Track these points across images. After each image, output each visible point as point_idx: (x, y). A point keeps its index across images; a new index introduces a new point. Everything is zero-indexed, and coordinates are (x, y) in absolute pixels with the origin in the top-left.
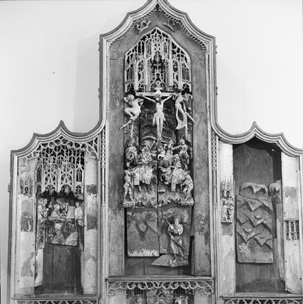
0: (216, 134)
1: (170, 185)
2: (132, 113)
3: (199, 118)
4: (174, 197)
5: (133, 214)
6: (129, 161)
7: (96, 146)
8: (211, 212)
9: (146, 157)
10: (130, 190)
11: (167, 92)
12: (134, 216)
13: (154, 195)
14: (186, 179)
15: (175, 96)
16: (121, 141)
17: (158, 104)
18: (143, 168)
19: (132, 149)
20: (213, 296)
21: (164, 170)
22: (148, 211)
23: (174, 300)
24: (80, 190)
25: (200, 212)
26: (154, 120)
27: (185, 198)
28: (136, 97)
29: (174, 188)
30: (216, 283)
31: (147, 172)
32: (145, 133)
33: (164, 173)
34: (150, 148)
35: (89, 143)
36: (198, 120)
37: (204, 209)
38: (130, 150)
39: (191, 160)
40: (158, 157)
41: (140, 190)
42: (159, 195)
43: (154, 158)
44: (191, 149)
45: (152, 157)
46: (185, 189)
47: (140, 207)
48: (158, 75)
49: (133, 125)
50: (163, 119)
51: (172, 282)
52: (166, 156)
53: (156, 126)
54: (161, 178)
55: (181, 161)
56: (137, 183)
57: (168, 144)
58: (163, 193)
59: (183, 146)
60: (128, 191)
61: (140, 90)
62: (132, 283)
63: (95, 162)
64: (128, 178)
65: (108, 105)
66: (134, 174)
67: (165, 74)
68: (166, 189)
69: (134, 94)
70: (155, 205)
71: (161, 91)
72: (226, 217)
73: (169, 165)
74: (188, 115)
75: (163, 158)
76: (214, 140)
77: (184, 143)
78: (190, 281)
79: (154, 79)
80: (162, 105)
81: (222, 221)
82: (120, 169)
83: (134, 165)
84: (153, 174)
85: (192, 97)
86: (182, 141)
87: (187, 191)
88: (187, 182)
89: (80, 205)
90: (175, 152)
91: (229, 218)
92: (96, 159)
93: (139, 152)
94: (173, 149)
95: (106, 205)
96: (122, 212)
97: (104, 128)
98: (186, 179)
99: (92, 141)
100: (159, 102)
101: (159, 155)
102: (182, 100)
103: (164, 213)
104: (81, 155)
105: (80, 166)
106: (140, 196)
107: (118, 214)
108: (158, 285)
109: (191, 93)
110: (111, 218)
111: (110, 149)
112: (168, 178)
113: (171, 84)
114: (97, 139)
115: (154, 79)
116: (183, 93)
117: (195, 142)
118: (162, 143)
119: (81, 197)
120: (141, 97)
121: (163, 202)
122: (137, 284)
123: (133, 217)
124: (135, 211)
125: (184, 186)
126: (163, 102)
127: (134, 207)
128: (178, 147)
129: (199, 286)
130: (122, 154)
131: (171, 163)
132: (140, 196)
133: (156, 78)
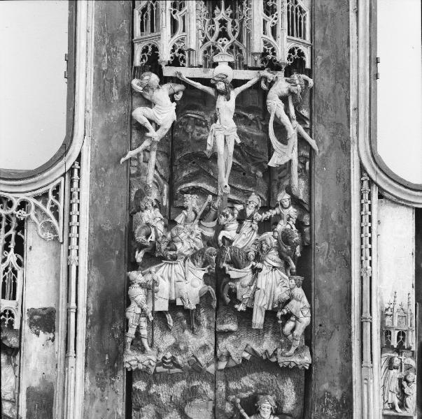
0: (371, 182)
1: (250, 311)
2: (151, 121)
3: (327, 138)
5: (148, 388)
6: (141, 247)
7: (56, 207)
8: (356, 387)
9: (189, 238)
10: (144, 325)
11: (246, 67)
12: (152, 391)
13: (206, 337)
14: (292, 297)
15: (266, 78)
16: (123, 193)
17: (221, 99)
18: (178, 267)
19: (151, 216)
21: (234, 274)
22: (189, 381)
24: (11, 323)
25: (326, 386)
26: (209, 141)
27: (289, 349)
28: (164, 80)
29: (258, 319)
31: (190, 276)
32: (185, 174)
33: (234, 280)
34: (200, 214)
35: (37, 198)
36: (327, 143)
37: (337, 378)
38: (145, 219)
39: (307, 248)
40: (220, 238)
41: (171, 323)
43: (210, 242)
44: (306, 219)
45: (203, 237)
46: (289, 325)
47: (167, 372)
48: (223, 22)
49: (153, 154)
50: (234, 138)
52: (242, 238)
53: (215, 157)
54: (226, 295)
55: (279, 250)
56: (162, 306)
57: (246, 205)
58: (228, 333)
59: (285, 212)
60: (138, 328)
61: (175, 62)
63: (52, 246)
64: (137, 293)
65: (90, 97)
66: (155, 282)
67: (241, 23)
68: (239, 325)
69: (158, 70)
70: (208, 365)
71: (230, 64)
72: (397, 402)
73: (247, 260)
74: (301, 128)
75: (231, 242)
76: (366, 196)
77: (287, 203)
79: (212, 33)
80: (232, 104)
81: (386, 412)
82: (119, 267)
83: (154, 257)
84: (207, 284)
85: (311, 81)
86: (284, 197)
87: (294, 329)
88: (294, 306)
89: (9, 362)
90: (266, 226)
91: (403, 405)
92: (56, 239)
93: (170, 223)
94: (259, 217)
95: (78, 363)
96: (120, 383)
97: (79, 159)
98: (292, 297)
99: (46, 195)
100: (226, 94)
101: (223, 233)
102: (285, 91)
103: (232, 385)
104: (17, 229)
105: (12, 257)
106: (169, 340)
107: (108, 388)
109: (309, 73)
110: (89, 397)
111: (93, 215)
112: (243, 294)
113: (258, 47)
114: (58, 187)
115: (212, 33)
116: (288, 73)
117: (318, 201)
118: (230, 201)
119: (12, 341)
120: (176, 80)
121: (229, 356)
123: (150, 396)
124: (155, 378)
125: (287, 317)
126: (234, 94)
128: (271, 213)
130: (123, 230)
131: (252, 254)
132: (169, 340)
133: (218, 30)
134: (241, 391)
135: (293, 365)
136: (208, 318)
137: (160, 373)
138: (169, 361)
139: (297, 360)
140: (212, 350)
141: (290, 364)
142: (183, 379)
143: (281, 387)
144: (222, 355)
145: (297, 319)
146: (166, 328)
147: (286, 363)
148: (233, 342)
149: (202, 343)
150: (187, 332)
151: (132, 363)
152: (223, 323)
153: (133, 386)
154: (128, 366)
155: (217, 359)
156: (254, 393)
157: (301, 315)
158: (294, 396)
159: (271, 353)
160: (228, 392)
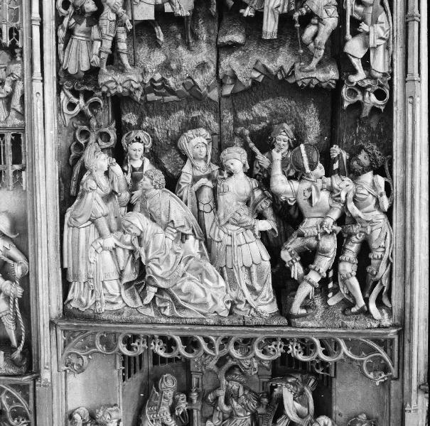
1: (259, 16)
4: (273, 60)
10: (123, 37)
13: (204, 53)
20: (395, 386)
22: (188, 112)
23: (272, 388)
29: (270, 26)
30: (407, 345)
41: (162, 38)
42: (222, 55)
46: (310, 31)
51: (260, 338)
58: (232, 47)
60: (115, 41)
62: (135, 337)
68: (247, 37)
78: (321, 336)
87: (316, 35)
103: (242, 116)
106: (159, 57)
108: (217, 347)
121: (235, 78)
122: (149, 339)
124: (146, 109)
125: (307, 19)
127: (138, 95)
129: (349, 354)
132: (159, 57)
134: (254, 122)
135: (315, 82)
136: (208, 32)
137: (153, 102)
138: (160, 84)
139: (320, 76)
140: (213, 69)
141: (311, 82)
142: (180, 108)
143: (302, 115)
144: (225, 76)
145: (320, 20)
146: (155, 44)
147: (307, 81)
148: (238, 58)
149: (200, 60)
150: (180, 48)
151: (109, 85)
152: (226, 33)
153: (123, 119)
154: (105, 89)
155: (221, 83)
156: (270, 124)
157: (325, 15)
158: (318, 126)
159: (287, 69)
160: (237, 123)
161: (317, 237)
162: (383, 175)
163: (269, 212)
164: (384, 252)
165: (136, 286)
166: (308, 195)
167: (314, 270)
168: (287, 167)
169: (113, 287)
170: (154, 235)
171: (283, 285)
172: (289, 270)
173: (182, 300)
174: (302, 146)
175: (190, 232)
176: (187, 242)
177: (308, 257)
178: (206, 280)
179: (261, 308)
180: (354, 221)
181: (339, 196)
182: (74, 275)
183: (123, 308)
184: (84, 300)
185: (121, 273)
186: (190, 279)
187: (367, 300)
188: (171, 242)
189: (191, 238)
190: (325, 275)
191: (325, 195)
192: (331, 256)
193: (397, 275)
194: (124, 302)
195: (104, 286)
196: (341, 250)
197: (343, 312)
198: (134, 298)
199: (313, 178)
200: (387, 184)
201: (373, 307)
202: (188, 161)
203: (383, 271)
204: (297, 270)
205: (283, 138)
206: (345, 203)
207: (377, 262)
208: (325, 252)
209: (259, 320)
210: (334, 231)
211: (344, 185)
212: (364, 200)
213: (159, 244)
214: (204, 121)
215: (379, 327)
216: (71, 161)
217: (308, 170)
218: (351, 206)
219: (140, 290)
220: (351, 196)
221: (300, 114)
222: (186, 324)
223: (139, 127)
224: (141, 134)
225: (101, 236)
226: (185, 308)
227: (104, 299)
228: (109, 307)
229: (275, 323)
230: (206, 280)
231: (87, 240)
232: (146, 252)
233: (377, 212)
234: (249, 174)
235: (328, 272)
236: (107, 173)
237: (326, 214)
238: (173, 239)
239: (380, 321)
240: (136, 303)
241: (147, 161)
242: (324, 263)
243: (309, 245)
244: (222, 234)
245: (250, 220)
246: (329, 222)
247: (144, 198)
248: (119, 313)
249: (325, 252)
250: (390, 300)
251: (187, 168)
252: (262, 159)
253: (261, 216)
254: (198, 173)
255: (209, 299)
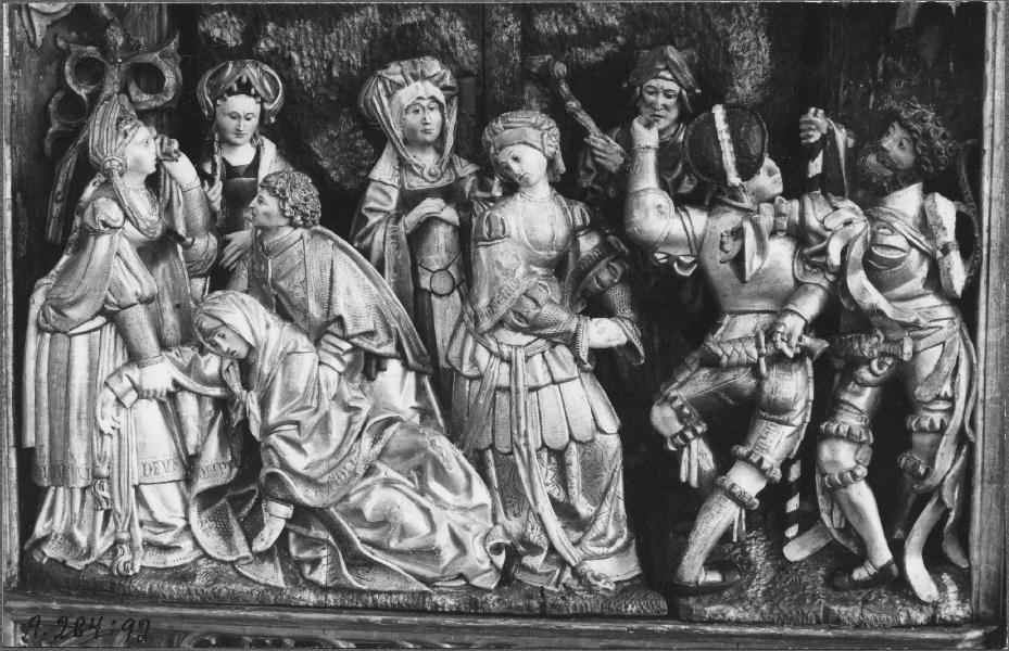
158: (764, 54)
161: (754, 368)
162: (952, 194)
163: (618, 296)
164: (950, 412)
165: (232, 500)
166: (732, 247)
167: (746, 459)
168: (674, 168)
169: (167, 502)
170: (286, 357)
171: (659, 504)
172: (674, 461)
173: (364, 542)
174: (719, 112)
175: (390, 349)
176: (380, 377)
177: (732, 420)
178: (434, 486)
179: (594, 567)
180: (867, 321)
181: (824, 252)
182: (53, 468)
183: (195, 562)
184: (81, 537)
185: (190, 465)
186: (388, 483)
187: (897, 548)
188: (333, 376)
189: (394, 366)
190: (777, 475)
191: (781, 252)
192: (797, 421)
193: (987, 477)
194: (197, 545)
195: (141, 500)
196: (826, 404)
197: (829, 581)
198: (226, 534)
199: (747, 203)
200: (961, 219)
201: (915, 568)
202: (388, 150)
203: (946, 463)
204: (697, 459)
205: (664, 89)
206: (841, 273)
207: (927, 439)
208: (778, 411)
209: (582, 600)
210: (805, 352)
211: (838, 220)
212: (893, 263)
213: (300, 383)
214: (435, 35)
215: (933, 623)
216: (48, 145)
217: (734, 179)
218: (857, 281)
219: (245, 512)
220: (857, 252)
221: (714, 21)
222: (376, 609)
223: (246, 52)
224: (252, 72)
225: (134, 357)
226: (371, 565)
227: (140, 535)
228: (152, 560)
229: (632, 609)
230: (434, 486)
231: (93, 368)
232: (264, 404)
233: (931, 300)
234: (565, 186)
235: (786, 465)
236: (153, 183)
237: (783, 302)
238: (341, 368)
239: (935, 605)
240: (231, 548)
241: (270, 149)
242: (776, 442)
243: (731, 390)
244: (483, 356)
245: (559, 316)
246: (793, 324)
247: (259, 251)
248: (181, 574)
249: (778, 411)
250: (965, 549)
251: (384, 170)
252: (605, 146)
253: (597, 307)
254: (416, 183)
255: (442, 539)
